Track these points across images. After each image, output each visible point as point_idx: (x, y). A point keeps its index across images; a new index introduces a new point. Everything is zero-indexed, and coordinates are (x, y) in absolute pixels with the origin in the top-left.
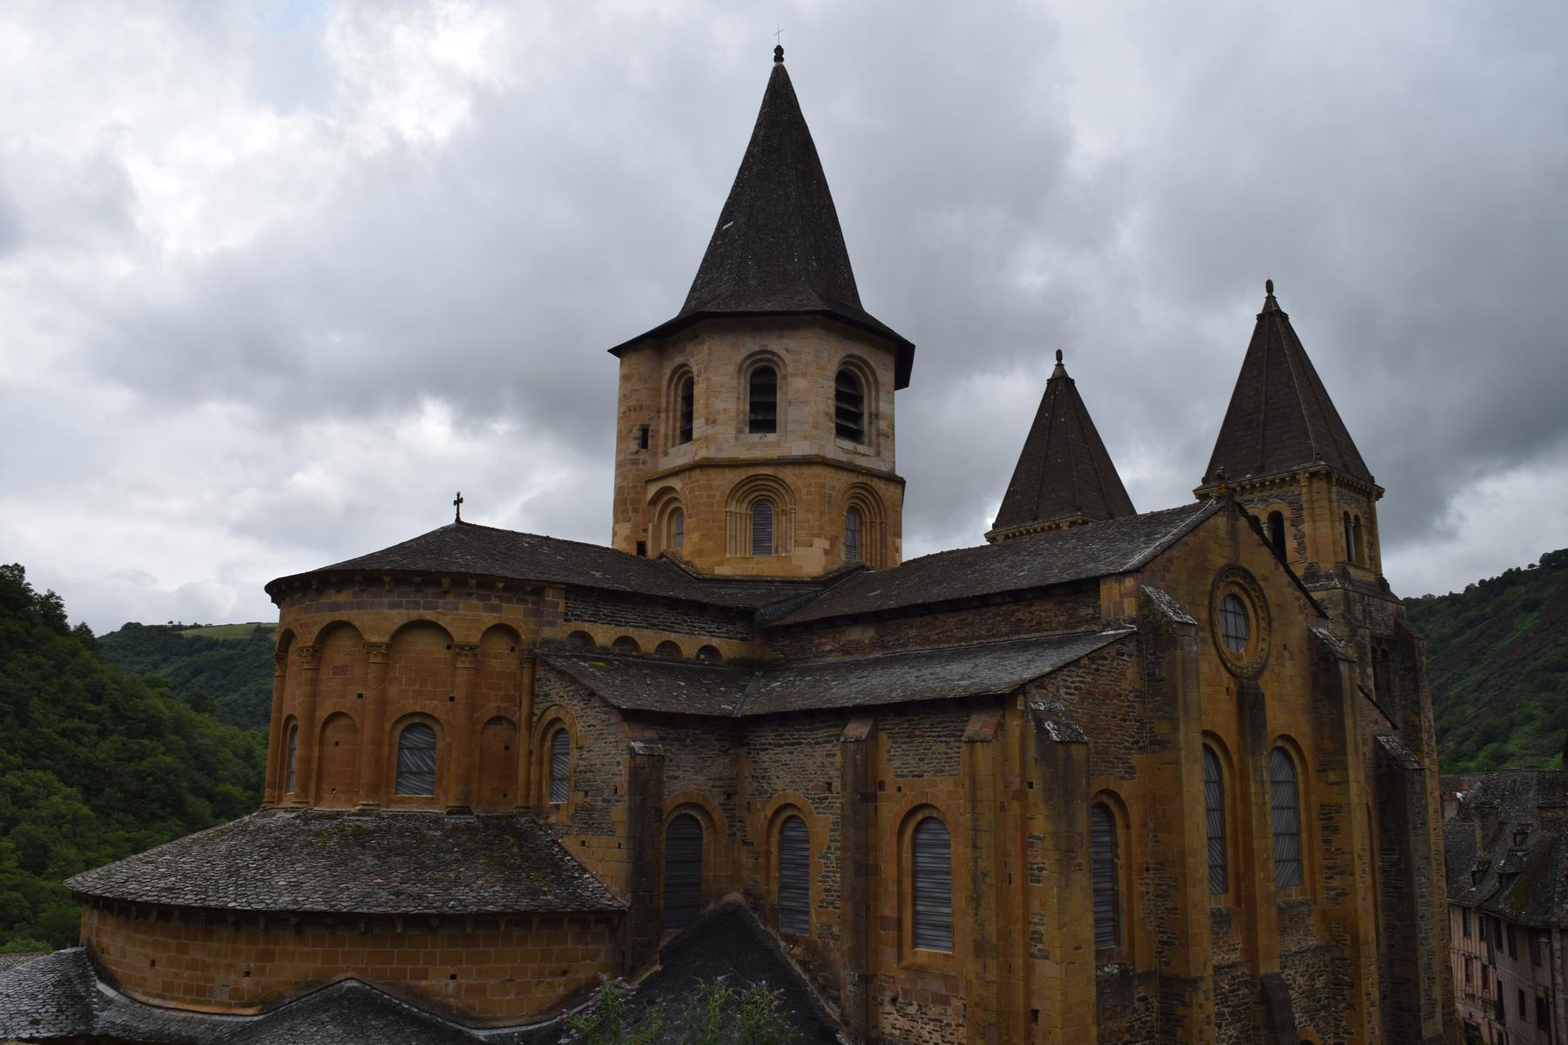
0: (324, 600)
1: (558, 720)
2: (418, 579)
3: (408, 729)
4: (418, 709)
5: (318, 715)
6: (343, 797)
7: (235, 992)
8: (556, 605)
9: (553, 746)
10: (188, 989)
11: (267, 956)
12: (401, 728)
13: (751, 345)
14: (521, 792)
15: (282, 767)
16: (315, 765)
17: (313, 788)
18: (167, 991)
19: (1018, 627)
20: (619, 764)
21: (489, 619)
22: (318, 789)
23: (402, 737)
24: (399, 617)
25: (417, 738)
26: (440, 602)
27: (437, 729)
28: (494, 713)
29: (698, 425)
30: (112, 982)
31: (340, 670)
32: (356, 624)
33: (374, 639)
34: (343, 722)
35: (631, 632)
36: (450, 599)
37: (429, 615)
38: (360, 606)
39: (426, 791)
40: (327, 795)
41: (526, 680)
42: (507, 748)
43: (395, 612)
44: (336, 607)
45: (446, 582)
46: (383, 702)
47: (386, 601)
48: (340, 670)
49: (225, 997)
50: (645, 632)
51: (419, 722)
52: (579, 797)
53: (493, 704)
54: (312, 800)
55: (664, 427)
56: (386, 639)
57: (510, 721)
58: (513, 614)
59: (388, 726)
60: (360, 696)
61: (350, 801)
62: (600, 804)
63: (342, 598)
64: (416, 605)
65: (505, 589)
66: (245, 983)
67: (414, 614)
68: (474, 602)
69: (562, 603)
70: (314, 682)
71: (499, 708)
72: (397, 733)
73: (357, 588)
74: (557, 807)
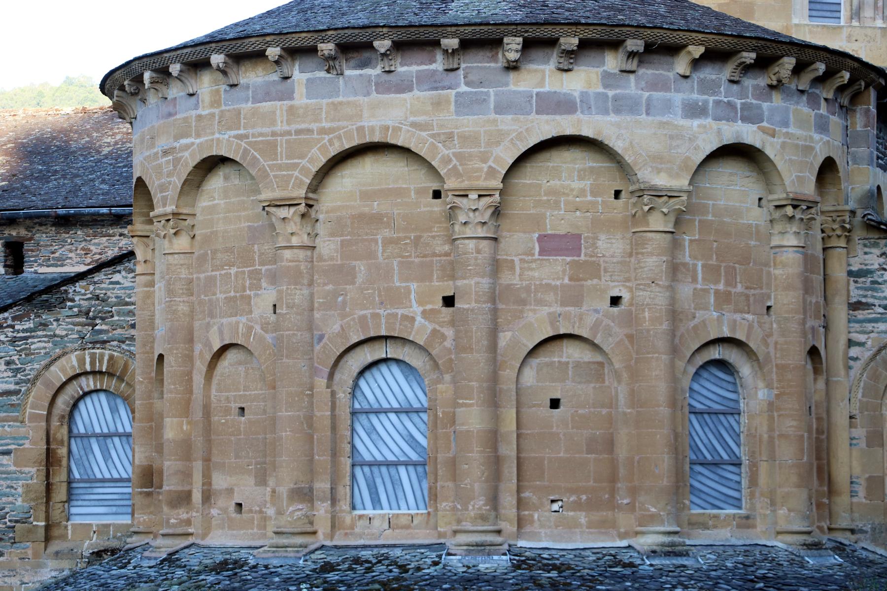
4: (726, 333)
5: (504, 338)
6: (583, 518)
15: (335, 454)
16: (508, 450)
17: (508, 501)
22: (521, 503)
25: (712, 391)
26: (765, 105)
27: (745, 370)
31: (551, 245)
32: (618, 146)
33: (661, 181)
34: (571, 352)
36: (777, 100)
37: (749, 134)
38: (623, 105)
43: (696, 123)
48: (551, 245)
56: (683, 182)
60: (615, 301)
61: (604, 526)
64: (727, 112)
73: (612, 62)
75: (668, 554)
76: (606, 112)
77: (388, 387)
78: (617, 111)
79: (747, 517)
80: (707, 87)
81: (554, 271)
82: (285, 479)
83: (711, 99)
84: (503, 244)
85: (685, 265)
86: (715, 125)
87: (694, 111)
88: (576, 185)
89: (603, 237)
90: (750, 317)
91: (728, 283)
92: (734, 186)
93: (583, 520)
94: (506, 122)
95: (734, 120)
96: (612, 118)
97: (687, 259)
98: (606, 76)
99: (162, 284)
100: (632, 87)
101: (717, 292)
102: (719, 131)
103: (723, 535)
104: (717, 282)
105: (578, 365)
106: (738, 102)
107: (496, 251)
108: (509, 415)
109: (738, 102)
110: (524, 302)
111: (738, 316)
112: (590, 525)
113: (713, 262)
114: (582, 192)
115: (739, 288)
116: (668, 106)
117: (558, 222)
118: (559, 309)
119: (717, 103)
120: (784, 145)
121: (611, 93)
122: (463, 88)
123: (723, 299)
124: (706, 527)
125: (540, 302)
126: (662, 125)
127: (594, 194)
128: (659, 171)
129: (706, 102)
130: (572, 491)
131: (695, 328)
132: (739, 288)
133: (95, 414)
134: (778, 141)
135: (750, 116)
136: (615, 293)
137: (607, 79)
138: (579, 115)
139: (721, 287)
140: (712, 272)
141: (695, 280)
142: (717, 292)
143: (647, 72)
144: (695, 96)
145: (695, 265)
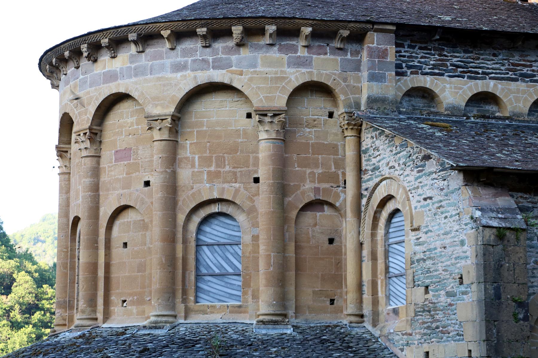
1: (389, 198)
2: (202, 31)
3: (206, 220)
4: (216, 195)
5: (102, 210)
8: (384, 54)
9: (387, 233)
12: (197, 219)
14: (351, 296)
16: (101, 273)
20: (462, 243)
21: (297, 77)
23: (199, 230)
25: (216, 231)
26: (234, 58)
27: (241, 218)
28: (312, 197)
35: (491, 86)
36: (245, 53)
38: (138, 72)
39: (231, 296)
40: (116, 309)
41: (350, 153)
42: (331, 241)
43: (179, 74)
45: (237, 30)
46: (172, 189)
47: (168, 62)
48: (124, 154)
50: (513, 85)
51: (213, 210)
53: (308, 185)
54: (100, 316)
56: (171, 110)
57: (331, 205)
58: (325, 65)
59: (181, 218)
62: (443, 300)
64: (204, 64)
65: (315, 35)
67: (204, 76)
68: (274, 54)
69: (392, 49)
70: (96, 172)
71: (317, 190)
72: (193, 227)
74: (396, 312)
75: (151, 328)
76: (130, 77)
78: (136, 75)
79: (240, 307)
80: (185, 53)
83: (190, 60)
84: (102, 160)
85: (186, 158)
86: (192, 74)
87: (178, 68)
88: (130, 120)
89: (141, 148)
90: (237, 185)
91: (217, 166)
92: (212, 108)
93: (135, 311)
95: (208, 69)
96: (134, 79)
97: (188, 155)
98: (132, 56)
100: (144, 60)
101: (209, 173)
102: (195, 77)
103: (216, 318)
104: (210, 166)
105: (135, 222)
106: (210, 59)
107: (98, 163)
108: (102, 252)
109: (210, 59)
110: (108, 190)
111: (226, 185)
112: (138, 314)
113: (207, 154)
114: (132, 123)
115: (227, 168)
116: (162, 68)
118: (121, 191)
119: (194, 61)
120: (251, 80)
121: (133, 66)
122: (81, 77)
123: (213, 176)
124: (205, 312)
125: (114, 189)
126: (159, 79)
127: (137, 124)
128: (156, 106)
129: (187, 62)
130: (131, 295)
131: (193, 195)
132: (227, 168)
134: (245, 78)
135: (218, 65)
136: (147, 179)
137: (132, 59)
138: (119, 81)
139: (213, 169)
140: (206, 161)
141: (193, 166)
142: (209, 173)
143: (150, 50)
144: (179, 59)
145: (193, 158)
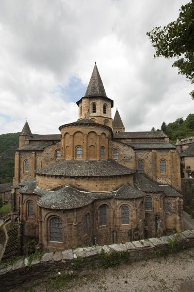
0: (89, 127)
7: (113, 188)
10: (105, 189)
11: (117, 182)
13: (105, 102)
18: (100, 190)
19: (153, 141)
24: (102, 132)
25: (102, 150)
29: (98, 111)
30: (84, 190)
31: (91, 139)
37: (104, 132)
40: (91, 158)
44: (92, 129)
49: (111, 189)
51: (103, 147)
52: (123, 158)
55: (91, 110)
63: (93, 127)
66: (114, 186)
77: (79, 149)
81: (91, 141)
82: (71, 155)
92: (103, 136)
94: (88, 130)
99: (62, 143)
117: (91, 137)
133: (58, 152)
